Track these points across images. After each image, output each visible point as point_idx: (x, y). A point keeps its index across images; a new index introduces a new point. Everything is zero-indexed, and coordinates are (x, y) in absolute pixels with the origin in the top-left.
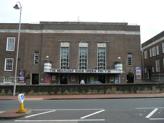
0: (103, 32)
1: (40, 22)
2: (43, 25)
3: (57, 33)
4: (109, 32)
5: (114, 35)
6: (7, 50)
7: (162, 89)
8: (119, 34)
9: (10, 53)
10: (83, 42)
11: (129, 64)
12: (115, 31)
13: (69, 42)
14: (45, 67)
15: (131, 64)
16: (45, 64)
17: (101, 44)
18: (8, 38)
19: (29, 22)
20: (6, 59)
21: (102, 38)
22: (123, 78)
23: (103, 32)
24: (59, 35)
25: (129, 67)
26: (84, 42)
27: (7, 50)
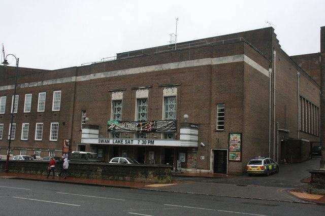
0: (172, 66)
1: (118, 54)
2: (126, 59)
3: (108, 76)
4: (183, 65)
5: (191, 69)
6: (53, 110)
7: (162, 177)
8: (198, 67)
9: (55, 115)
10: (141, 89)
11: (219, 127)
12: (193, 61)
13: (122, 91)
14: (83, 136)
15: (222, 127)
16: (84, 131)
17: (170, 89)
18: (39, 94)
19: (78, 64)
20: (51, 123)
21: (170, 79)
22: (203, 158)
23: (172, 66)
24: (110, 79)
25: (217, 134)
26: (142, 88)
27: (53, 110)
